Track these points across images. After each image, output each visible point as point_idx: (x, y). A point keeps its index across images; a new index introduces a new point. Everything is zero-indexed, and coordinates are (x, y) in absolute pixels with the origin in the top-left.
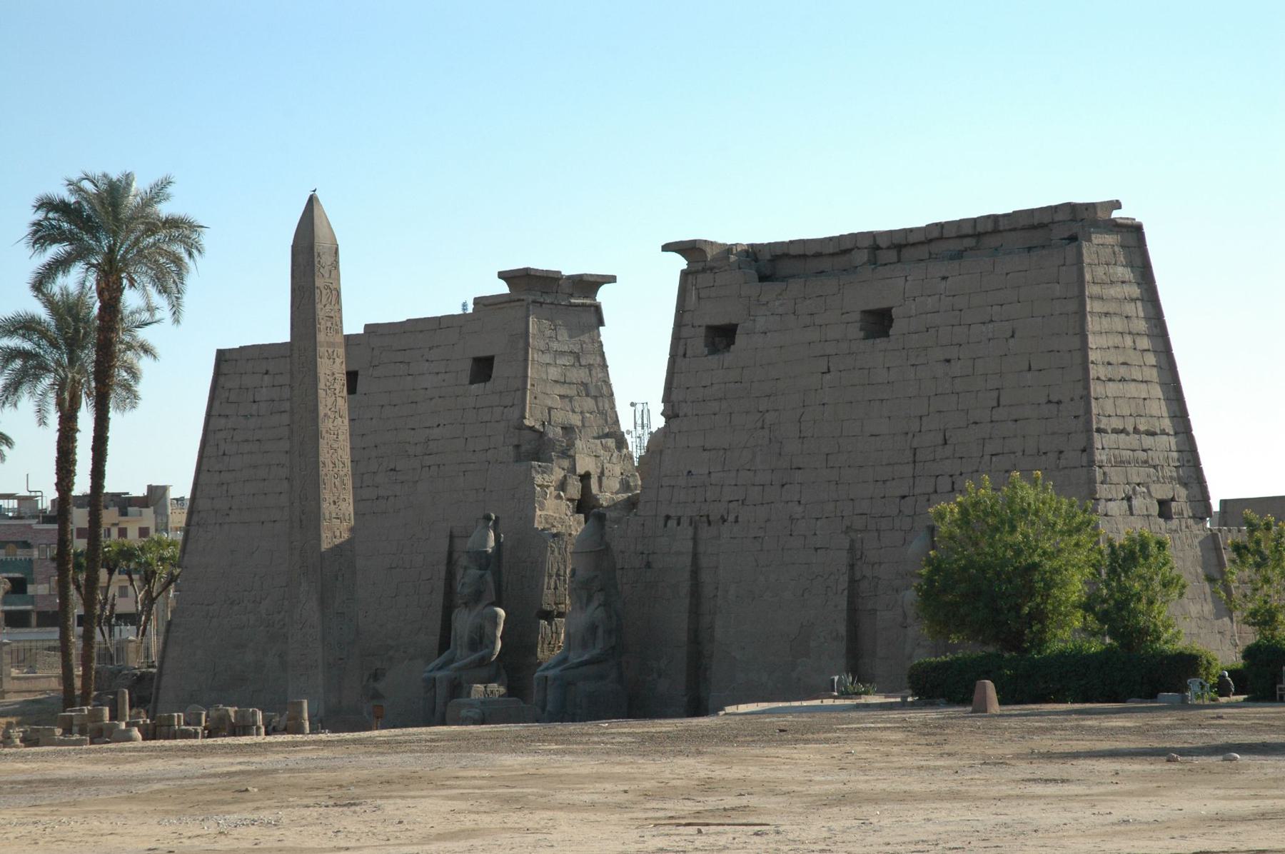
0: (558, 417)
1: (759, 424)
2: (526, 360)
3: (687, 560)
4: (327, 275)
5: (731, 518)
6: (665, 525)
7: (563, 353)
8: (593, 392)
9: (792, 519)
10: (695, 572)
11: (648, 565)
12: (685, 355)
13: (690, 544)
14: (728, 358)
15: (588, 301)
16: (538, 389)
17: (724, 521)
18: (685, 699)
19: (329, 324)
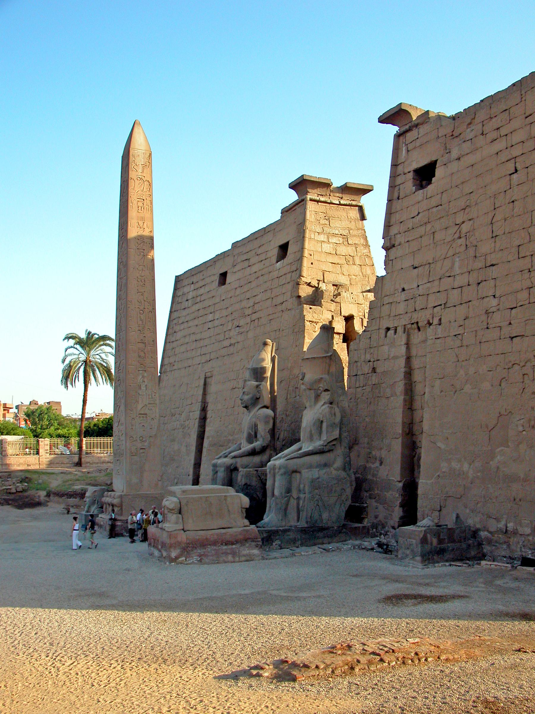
0: (329, 277)
1: (457, 236)
2: (304, 237)
3: (402, 362)
4: (140, 171)
5: (436, 321)
6: (386, 336)
7: (334, 235)
8: (358, 262)
9: (487, 313)
10: (409, 374)
11: (374, 370)
12: (398, 198)
13: (403, 349)
14: (430, 188)
15: (354, 203)
16: (316, 257)
17: (430, 324)
18: (401, 485)
19: (140, 204)
